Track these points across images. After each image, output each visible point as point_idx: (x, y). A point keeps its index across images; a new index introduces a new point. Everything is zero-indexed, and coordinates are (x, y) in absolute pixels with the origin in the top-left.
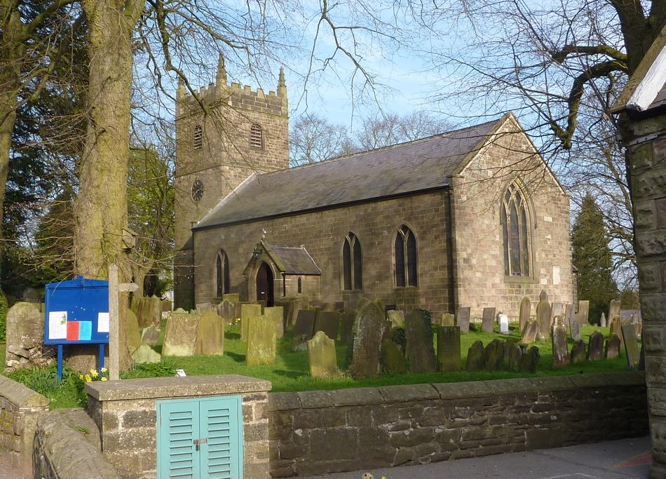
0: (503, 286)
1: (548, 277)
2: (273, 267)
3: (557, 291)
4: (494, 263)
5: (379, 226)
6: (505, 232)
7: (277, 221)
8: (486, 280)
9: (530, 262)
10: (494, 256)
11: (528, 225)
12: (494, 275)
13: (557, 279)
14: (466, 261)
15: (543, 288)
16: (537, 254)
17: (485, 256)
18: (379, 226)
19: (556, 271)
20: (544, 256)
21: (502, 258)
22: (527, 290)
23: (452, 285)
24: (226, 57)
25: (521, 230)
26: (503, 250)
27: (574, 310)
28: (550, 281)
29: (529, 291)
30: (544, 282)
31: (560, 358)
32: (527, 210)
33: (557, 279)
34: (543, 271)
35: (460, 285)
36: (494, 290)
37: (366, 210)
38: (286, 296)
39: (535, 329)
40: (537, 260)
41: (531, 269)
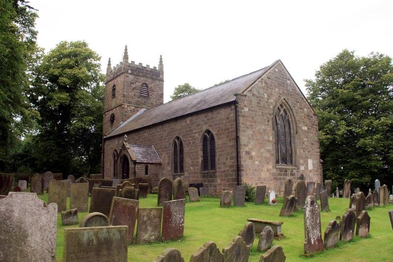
0: (274, 171)
1: (305, 165)
2: (129, 158)
3: (311, 174)
4: (268, 155)
5: (194, 131)
6: (277, 135)
7: (141, 132)
8: (263, 166)
9: (293, 155)
10: (268, 151)
11: (292, 131)
12: (268, 163)
13: (310, 167)
14: (248, 153)
15: (301, 172)
16: (298, 150)
17: (262, 150)
18: (194, 131)
19: (310, 162)
20: (302, 152)
21: (274, 152)
22: (291, 174)
23: (238, 169)
24: (243, 92)
25: (287, 135)
26: (275, 147)
27: (322, 186)
28: (307, 168)
29: (292, 174)
30: (302, 168)
31: (312, 241)
32: (291, 122)
33: (310, 167)
34: (301, 161)
35: (243, 170)
36: (268, 173)
37: (379, 121)
38: (136, 177)
39: (293, 203)
40: (298, 154)
41: (294, 160)
